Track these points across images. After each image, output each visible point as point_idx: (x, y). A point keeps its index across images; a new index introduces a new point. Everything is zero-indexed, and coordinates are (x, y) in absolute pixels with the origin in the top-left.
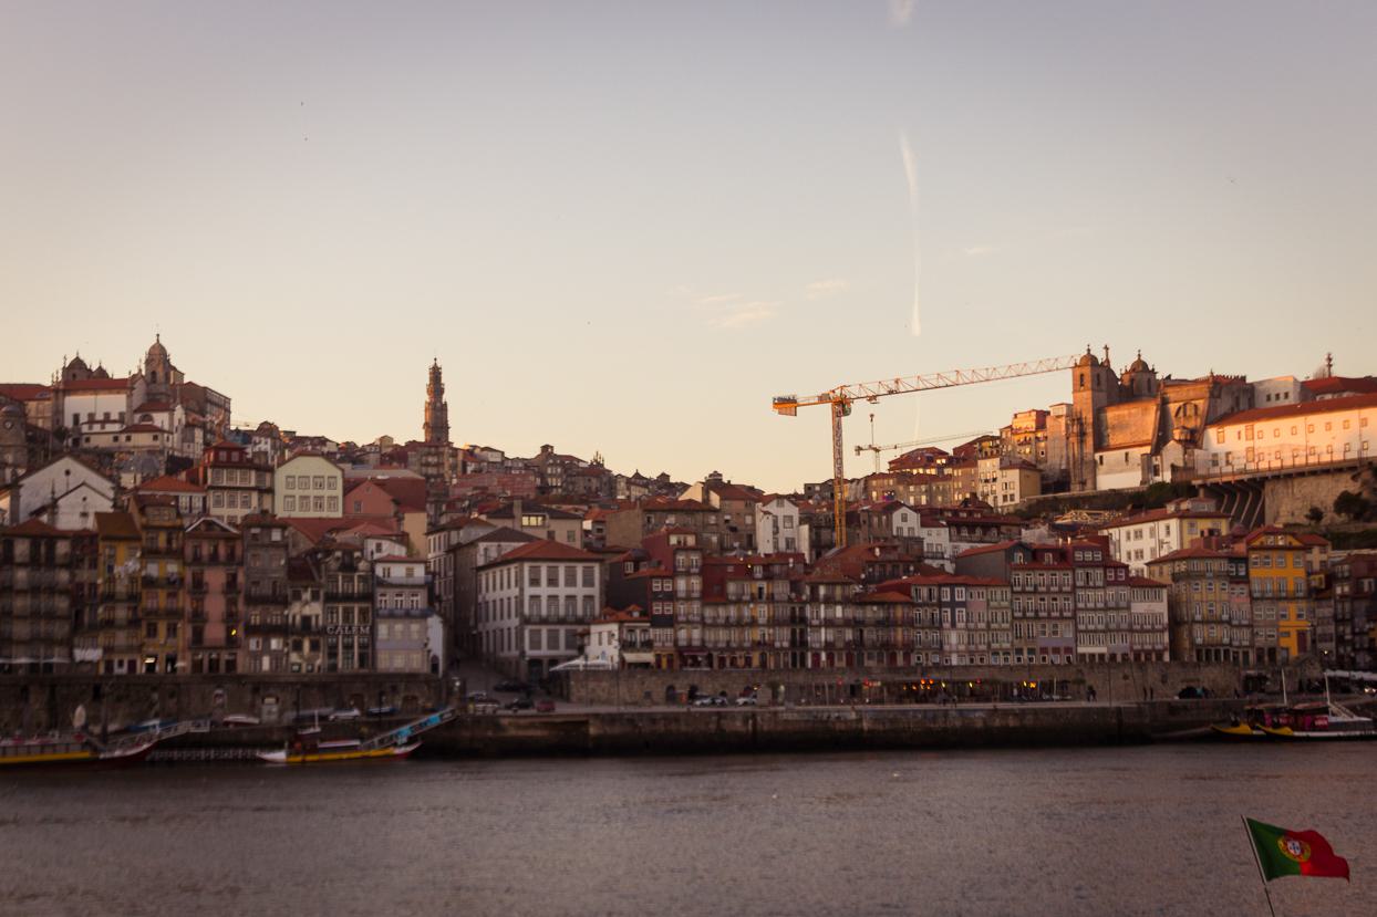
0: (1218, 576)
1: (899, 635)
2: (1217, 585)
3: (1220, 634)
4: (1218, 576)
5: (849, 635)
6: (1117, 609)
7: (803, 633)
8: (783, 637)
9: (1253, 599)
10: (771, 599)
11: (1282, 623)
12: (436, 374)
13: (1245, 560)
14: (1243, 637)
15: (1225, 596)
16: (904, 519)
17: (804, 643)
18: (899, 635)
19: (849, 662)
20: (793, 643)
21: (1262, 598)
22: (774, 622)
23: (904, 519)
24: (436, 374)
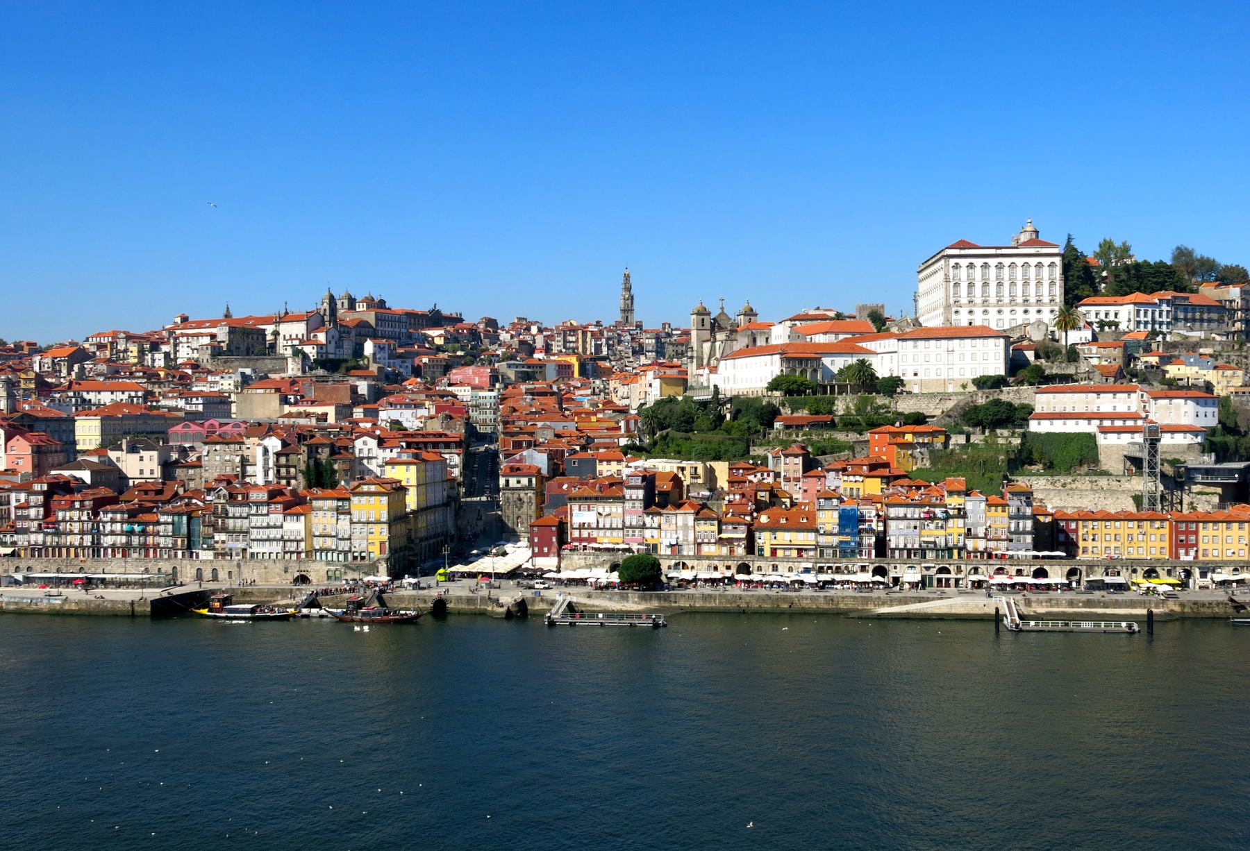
0: (330, 509)
1: (150, 540)
2: (329, 514)
3: (330, 543)
4: (330, 509)
5: (124, 539)
6: (275, 527)
7: (99, 539)
8: (88, 540)
9: (352, 522)
10: (80, 520)
11: (370, 536)
12: (627, 277)
13: (349, 499)
14: (344, 546)
15: (334, 520)
16: (365, 443)
17: (99, 543)
18: (150, 540)
19: (124, 556)
20: (93, 542)
21: (359, 522)
22: (82, 533)
23: (365, 443)
24: (627, 277)
